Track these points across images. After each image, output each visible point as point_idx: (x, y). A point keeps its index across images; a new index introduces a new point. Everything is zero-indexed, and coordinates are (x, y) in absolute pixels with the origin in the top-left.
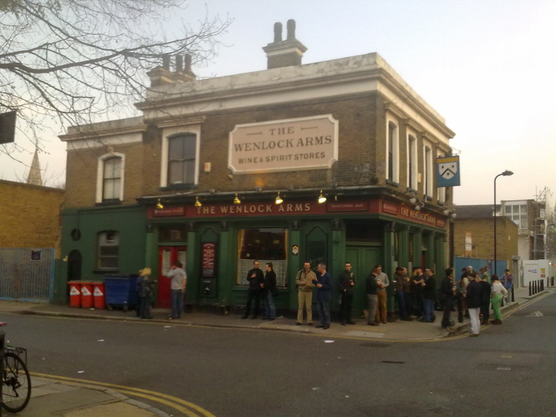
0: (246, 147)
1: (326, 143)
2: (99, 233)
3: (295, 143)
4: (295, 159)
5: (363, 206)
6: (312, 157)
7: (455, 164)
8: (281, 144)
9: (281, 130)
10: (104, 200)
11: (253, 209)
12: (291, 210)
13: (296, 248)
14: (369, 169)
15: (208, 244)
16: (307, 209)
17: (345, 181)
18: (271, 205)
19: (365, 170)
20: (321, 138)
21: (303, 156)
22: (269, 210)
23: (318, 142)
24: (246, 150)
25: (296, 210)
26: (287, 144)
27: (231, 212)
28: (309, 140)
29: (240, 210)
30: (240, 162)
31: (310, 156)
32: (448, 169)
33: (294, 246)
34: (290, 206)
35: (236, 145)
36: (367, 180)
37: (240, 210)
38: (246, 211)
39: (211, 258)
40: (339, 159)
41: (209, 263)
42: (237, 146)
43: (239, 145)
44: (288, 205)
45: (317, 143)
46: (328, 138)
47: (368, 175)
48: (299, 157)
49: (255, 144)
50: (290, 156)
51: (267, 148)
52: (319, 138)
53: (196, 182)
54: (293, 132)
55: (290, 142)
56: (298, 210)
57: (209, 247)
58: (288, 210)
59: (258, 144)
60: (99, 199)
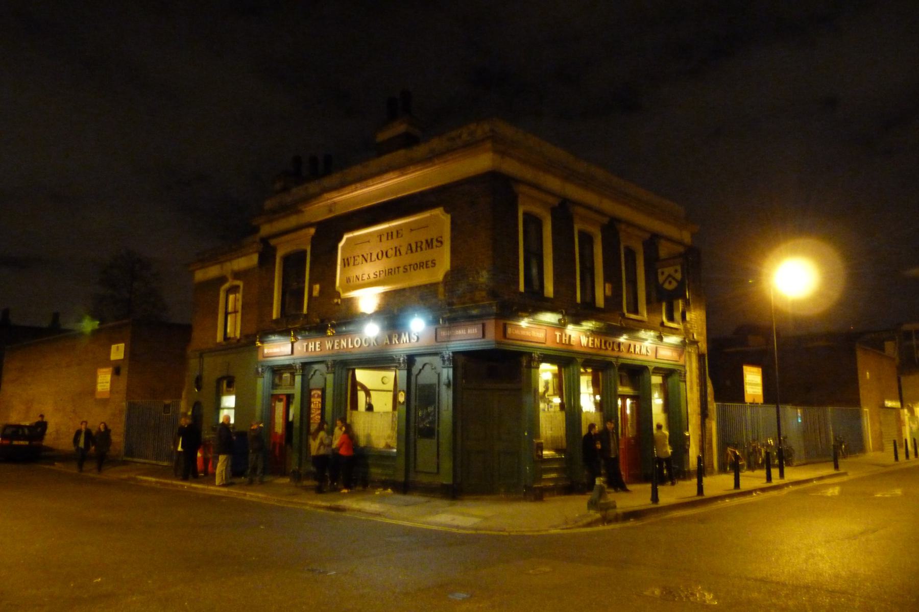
0: (354, 260)
1: (437, 246)
2: (219, 381)
3: (403, 250)
4: (404, 272)
5: (476, 331)
6: (421, 268)
7: (679, 268)
8: (389, 254)
9: (390, 234)
10: (226, 338)
13: (402, 395)
16: (414, 340)
20: (432, 240)
21: (412, 267)
23: (429, 246)
24: (354, 265)
25: (402, 342)
26: (396, 251)
28: (419, 244)
30: (347, 282)
31: (420, 266)
32: (670, 276)
33: (400, 391)
35: (344, 260)
36: (484, 294)
37: (345, 346)
38: (350, 346)
39: (319, 409)
40: (452, 266)
41: (316, 417)
42: (346, 260)
43: (348, 259)
45: (427, 248)
46: (439, 239)
47: (484, 286)
48: (408, 268)
49: (363, 256)
50: (398, 268)
51: (375, 260)
52: (429, 241)
53: (305, 311)
54: (402, 236)
55: (399, 250)
56: (405, 341)
57: (316, 395)
59: (365, 255)
60: (220, 337)
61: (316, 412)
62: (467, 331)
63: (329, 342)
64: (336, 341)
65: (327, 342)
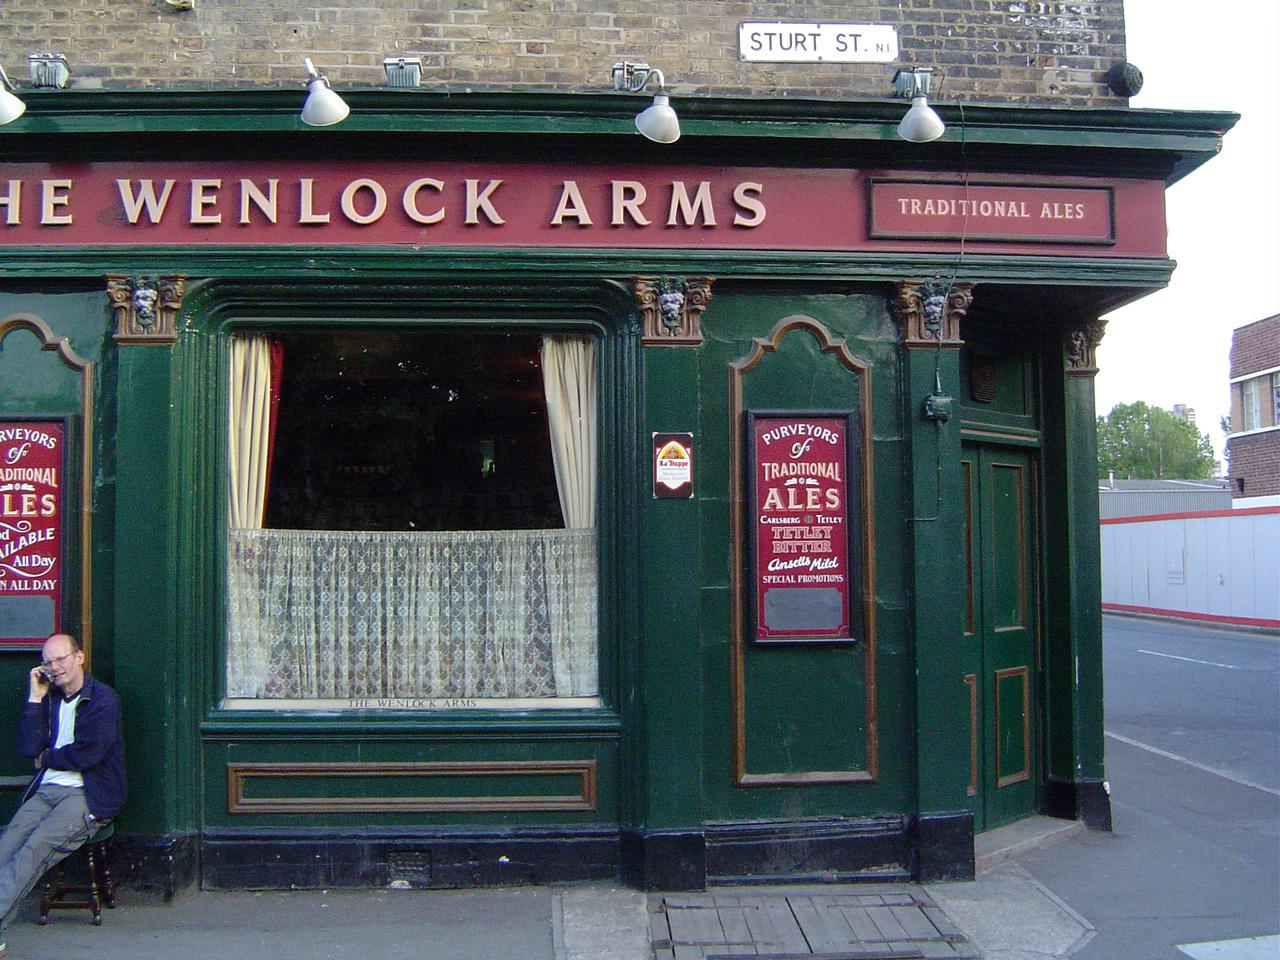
11: (366, 196)
12: (640, 219)
14: (1090, 21)
15: (16, 433)
17: (957, 72)
18: (494, 184)
19: (1067, 26)
22: (480, 210)
25: (673, 221)
27: (197, 216)
29: (270, 209)
34: (629, 193)
36: (1083, 78)
38: (307, 216)
41: (25, 562)
44: (619, 187)
56: (690, 218)
58: (618, 218)
61: (15, 537)
62: (1034, 209)
63: (147, 185)
64: (197, 185)
65: (124, 185)
